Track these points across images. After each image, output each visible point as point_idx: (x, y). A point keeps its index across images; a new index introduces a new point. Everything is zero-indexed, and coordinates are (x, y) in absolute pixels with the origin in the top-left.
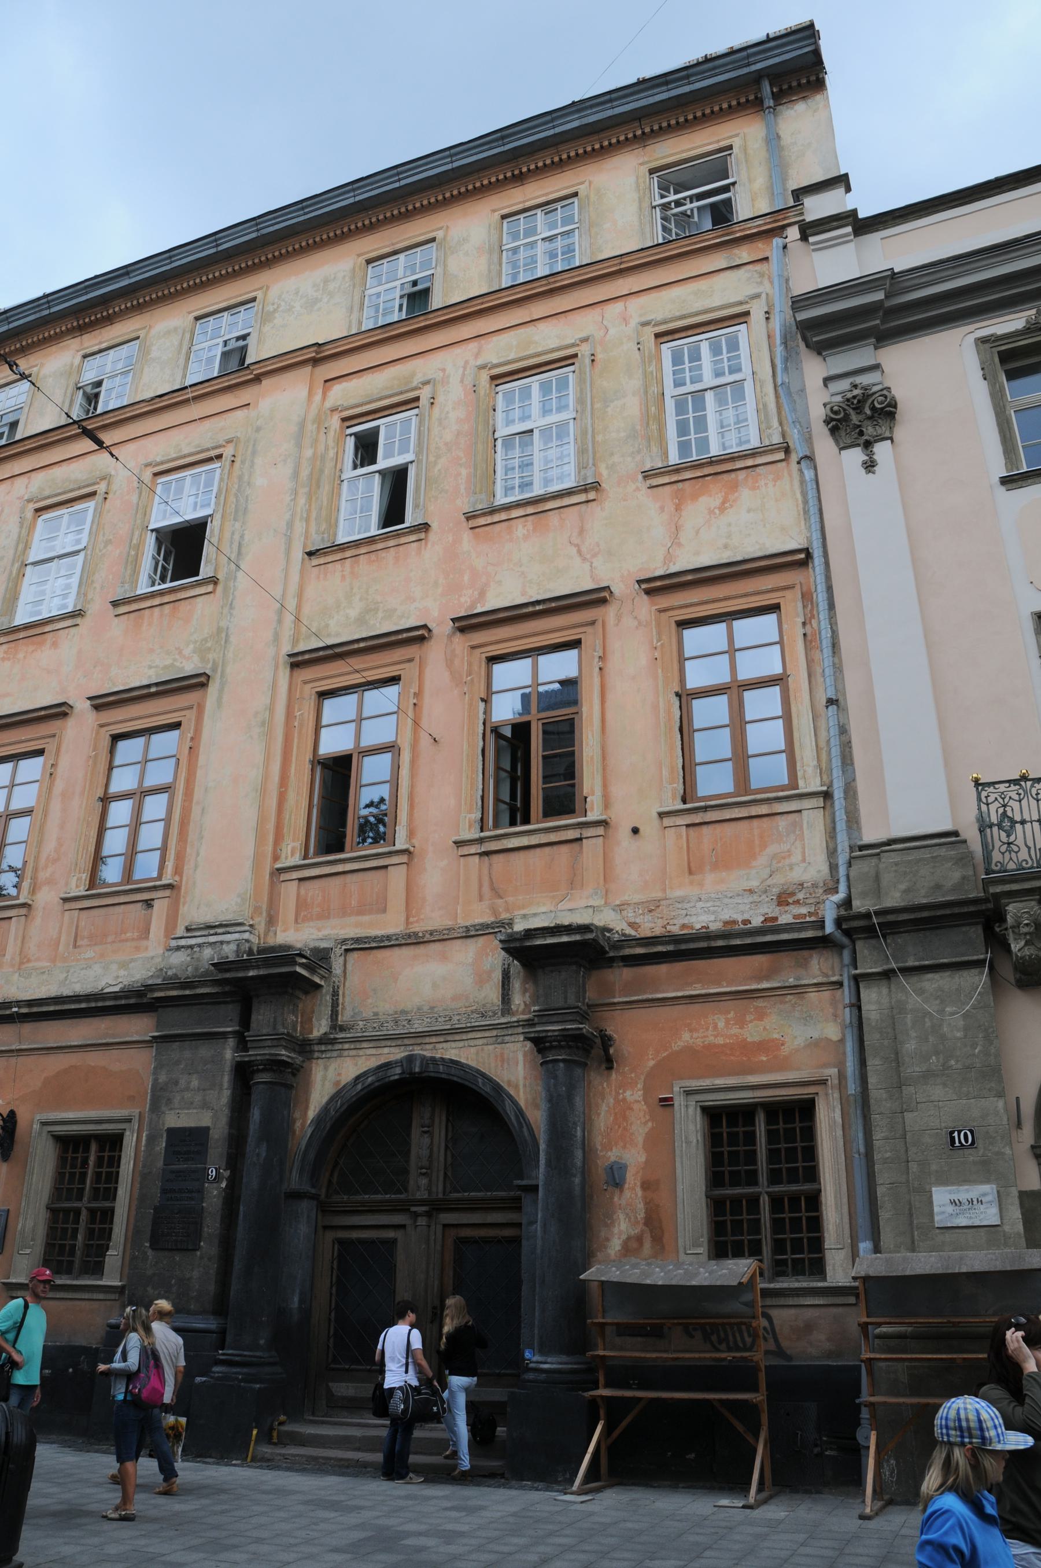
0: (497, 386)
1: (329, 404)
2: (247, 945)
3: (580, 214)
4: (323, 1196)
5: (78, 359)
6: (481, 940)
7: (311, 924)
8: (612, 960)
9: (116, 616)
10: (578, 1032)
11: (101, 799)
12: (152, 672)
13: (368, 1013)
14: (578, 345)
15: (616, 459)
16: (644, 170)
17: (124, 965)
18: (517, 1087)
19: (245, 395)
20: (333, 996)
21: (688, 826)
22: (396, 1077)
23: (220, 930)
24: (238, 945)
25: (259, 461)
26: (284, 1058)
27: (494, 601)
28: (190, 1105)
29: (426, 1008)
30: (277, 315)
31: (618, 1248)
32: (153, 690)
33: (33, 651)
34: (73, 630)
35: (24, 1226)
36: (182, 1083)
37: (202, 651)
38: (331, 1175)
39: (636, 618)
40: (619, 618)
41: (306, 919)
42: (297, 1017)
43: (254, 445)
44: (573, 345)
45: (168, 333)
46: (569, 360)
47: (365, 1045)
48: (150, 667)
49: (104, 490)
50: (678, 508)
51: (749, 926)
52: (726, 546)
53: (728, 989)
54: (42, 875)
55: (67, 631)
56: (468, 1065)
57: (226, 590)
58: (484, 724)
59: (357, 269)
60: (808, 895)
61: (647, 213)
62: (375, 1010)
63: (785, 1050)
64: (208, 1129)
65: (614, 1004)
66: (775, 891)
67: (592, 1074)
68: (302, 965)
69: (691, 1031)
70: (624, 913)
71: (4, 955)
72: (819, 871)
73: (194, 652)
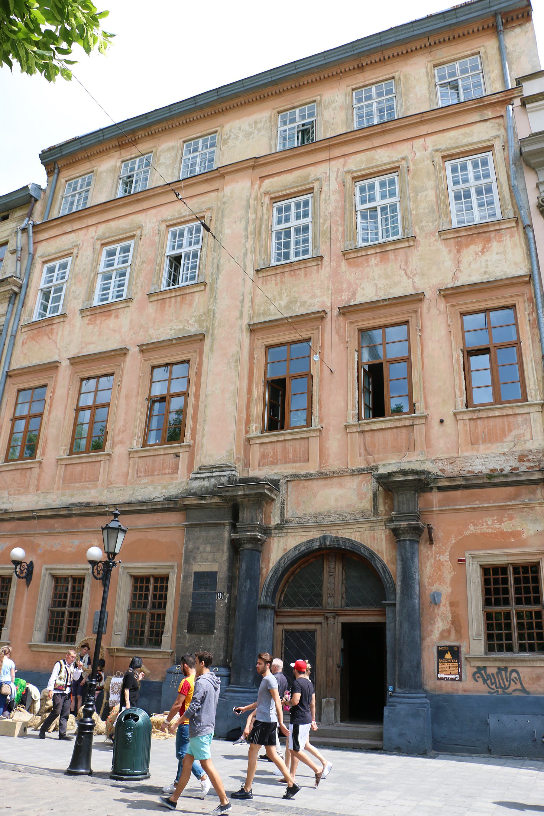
0: (355, 182)
1: (262, 190)
2: (234, 478)
3: (396, 88)
4: (277, 608)
5: (119, 163)
6: (361, 477)
7: (268, 467)
12: (172, 332)
13: (300, 514)
14: (400, 161)
15: (424, 223)
16: (430, 65)
18: (382, 553)
19: (216, 185)
20: (281, 504)
21: (469, 419)
22: (317, 547)
23: (218, 470)
24: (229, 478)
25: (226, 220)
27: (360, 299)
28: (206, 560)
30: (229, 141)
31: (438, 636)
32: (174, 342)
34: (127, 309)
35: (117, 620)
36: (202, 549)
37: (200, 322)
38: (281, 596)
39: (438, 309)
40: (429, 309)
41: (264, 464)
43: (223, 211)
44: (397, 161)
45: (169, 149)
46: (395, 169)
47: (299, 530)
48: (171, 330)
50: (459, 251)
51: (503, 472)
52: (485, 272)
53: (494, 505)
55: (123, 309)
57: (212, 289)
58: (358, 363)
59: (273, 117)
60: (534, 457)
61: (433, 89)
62: (304, 512)
63: (524, 536)
64: (216, 573)
65: (433, 511)
66: (517, 454)
67: (422, 547)
68: (267, 489)
69: (474, 525)
70: (437, 464)
72: (540, 445)
73: (195, 322)
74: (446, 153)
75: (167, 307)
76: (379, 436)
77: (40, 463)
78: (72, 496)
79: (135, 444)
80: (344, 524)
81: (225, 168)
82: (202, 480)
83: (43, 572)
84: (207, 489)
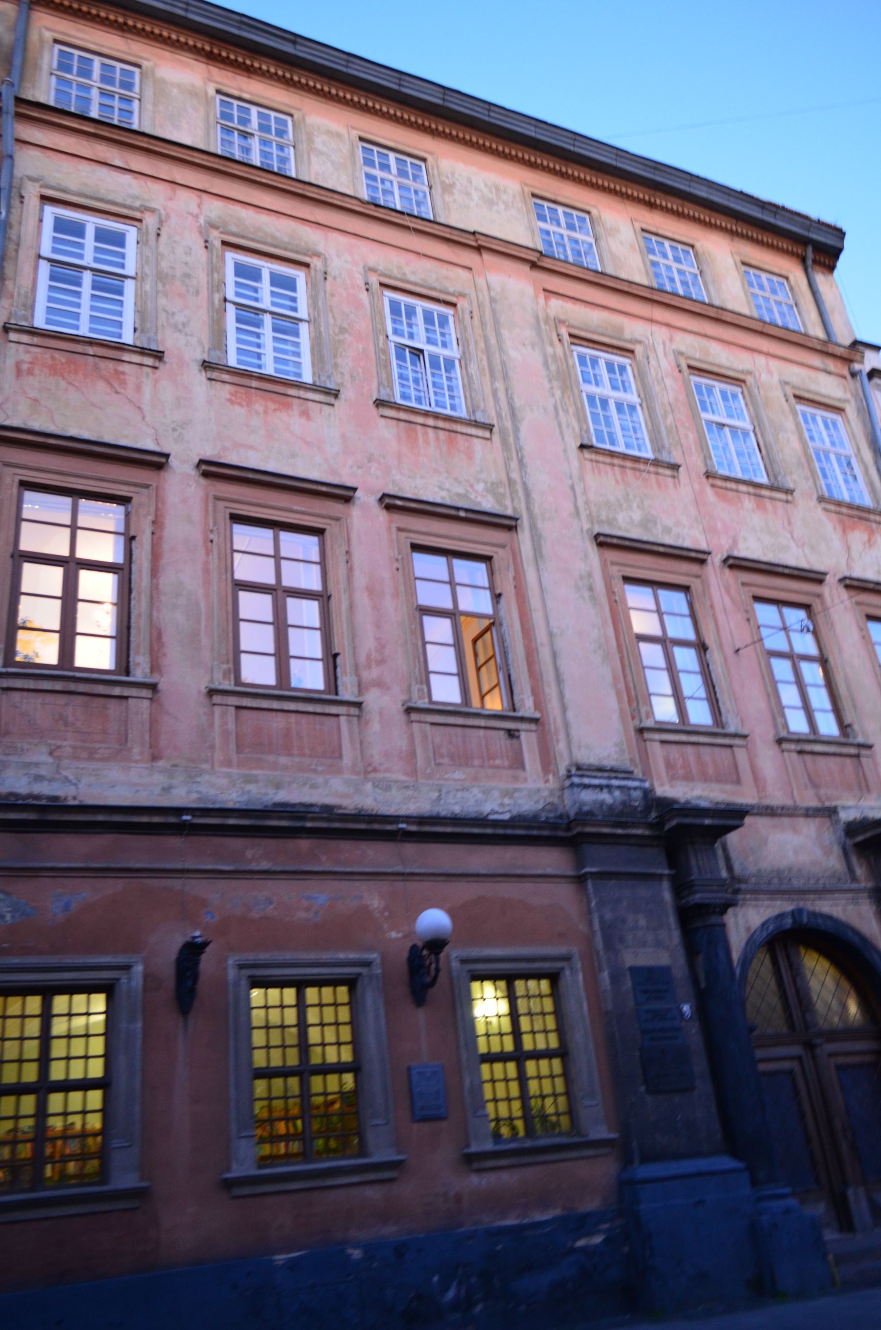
6: (817, 820)
13: (752, 869)
15: (795, 476)
17: (507, 793)
25: (505, 333)
32: (462, 514)
33: (275, 410)
34: (326, 408)
44: (742, 372)
49: (323, 269)
50: (844, 531)
54: (367, 675)
71: (340, 756)
73: (487, 490)
74: (798, 393)
75: (421, 440)
76: (821, 760)
78: (278, 786)
80: (823, 892)
81: (488, 239)
82: (598, 790)
83: (232, 974)
84: (611, 807)
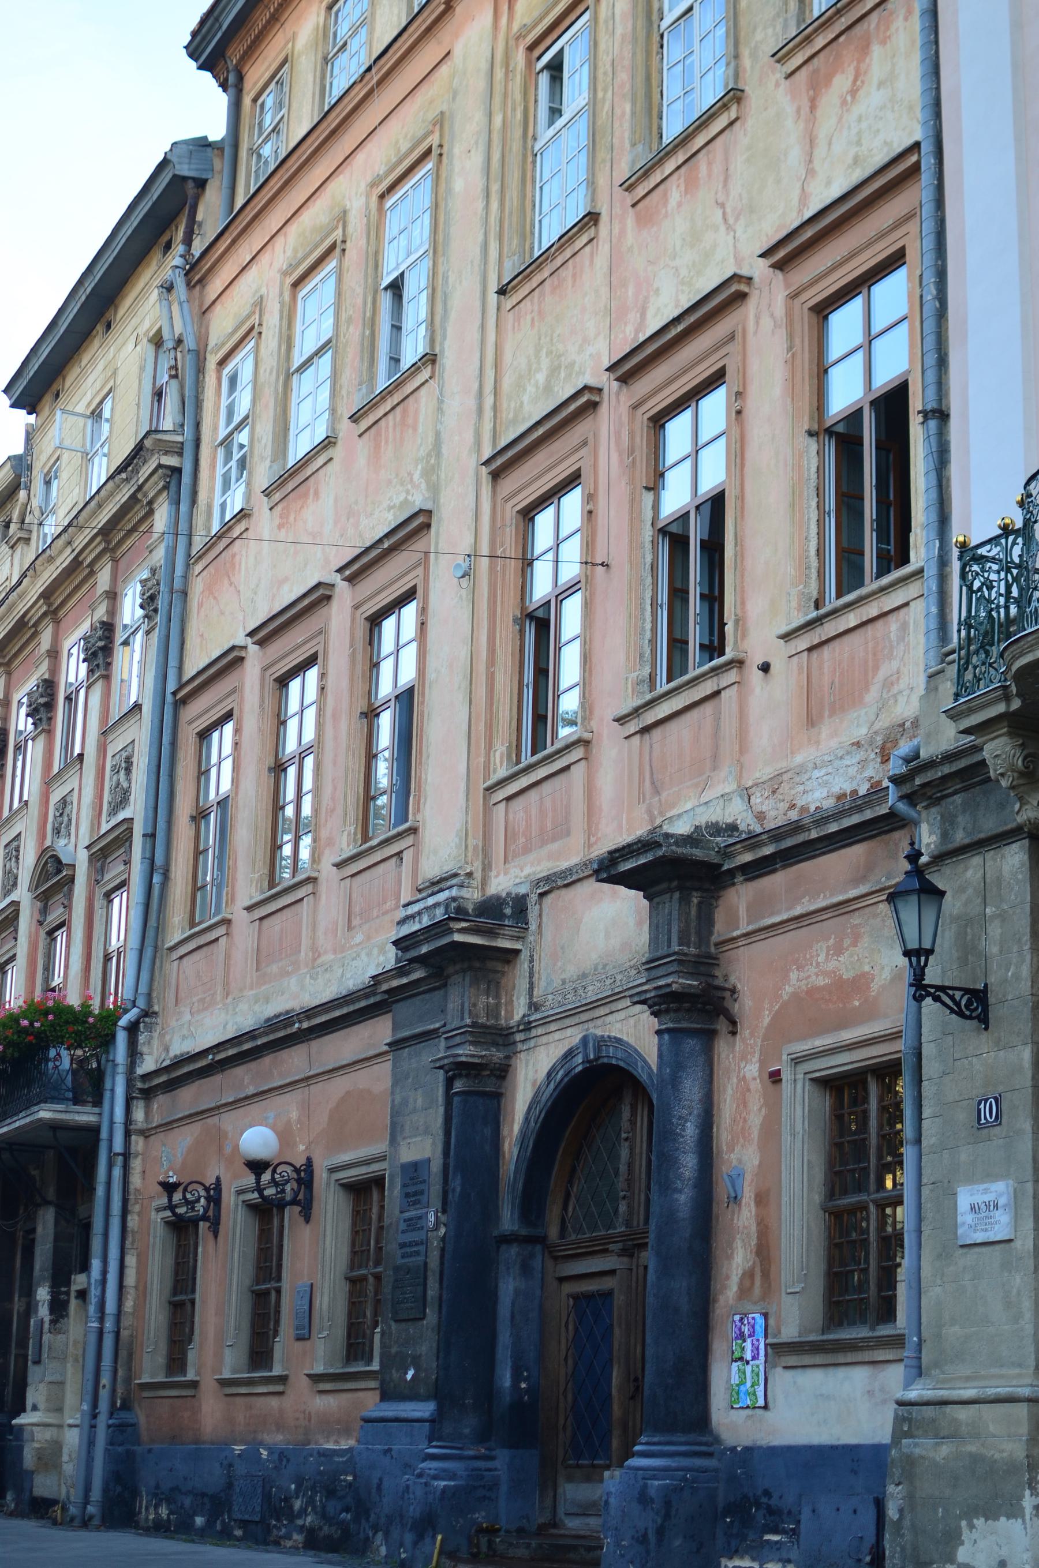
1: (515, 27)
2: (453, 905)
8: (732, 873)
9: (360, 436)
10: (668, 990)
11: (364, 715)
13: (557, 983)
21: (810, 650)
22: (580, 1068)
26: (464, 1059)
29: (600, 967)
34: (329, 466)
36: (411, 1100)
38: (565, 1208)
42: (497, 997)
47: (553, 1027)
48: (390, 508)
52: (856, 160)
56: (628, 1043)
62: (563, 976)
63: (875, 986)
64: (429, 1160)
66: (879, 740)
77: (227, 922)
78: (267, 1000)
79: (344, 845)
